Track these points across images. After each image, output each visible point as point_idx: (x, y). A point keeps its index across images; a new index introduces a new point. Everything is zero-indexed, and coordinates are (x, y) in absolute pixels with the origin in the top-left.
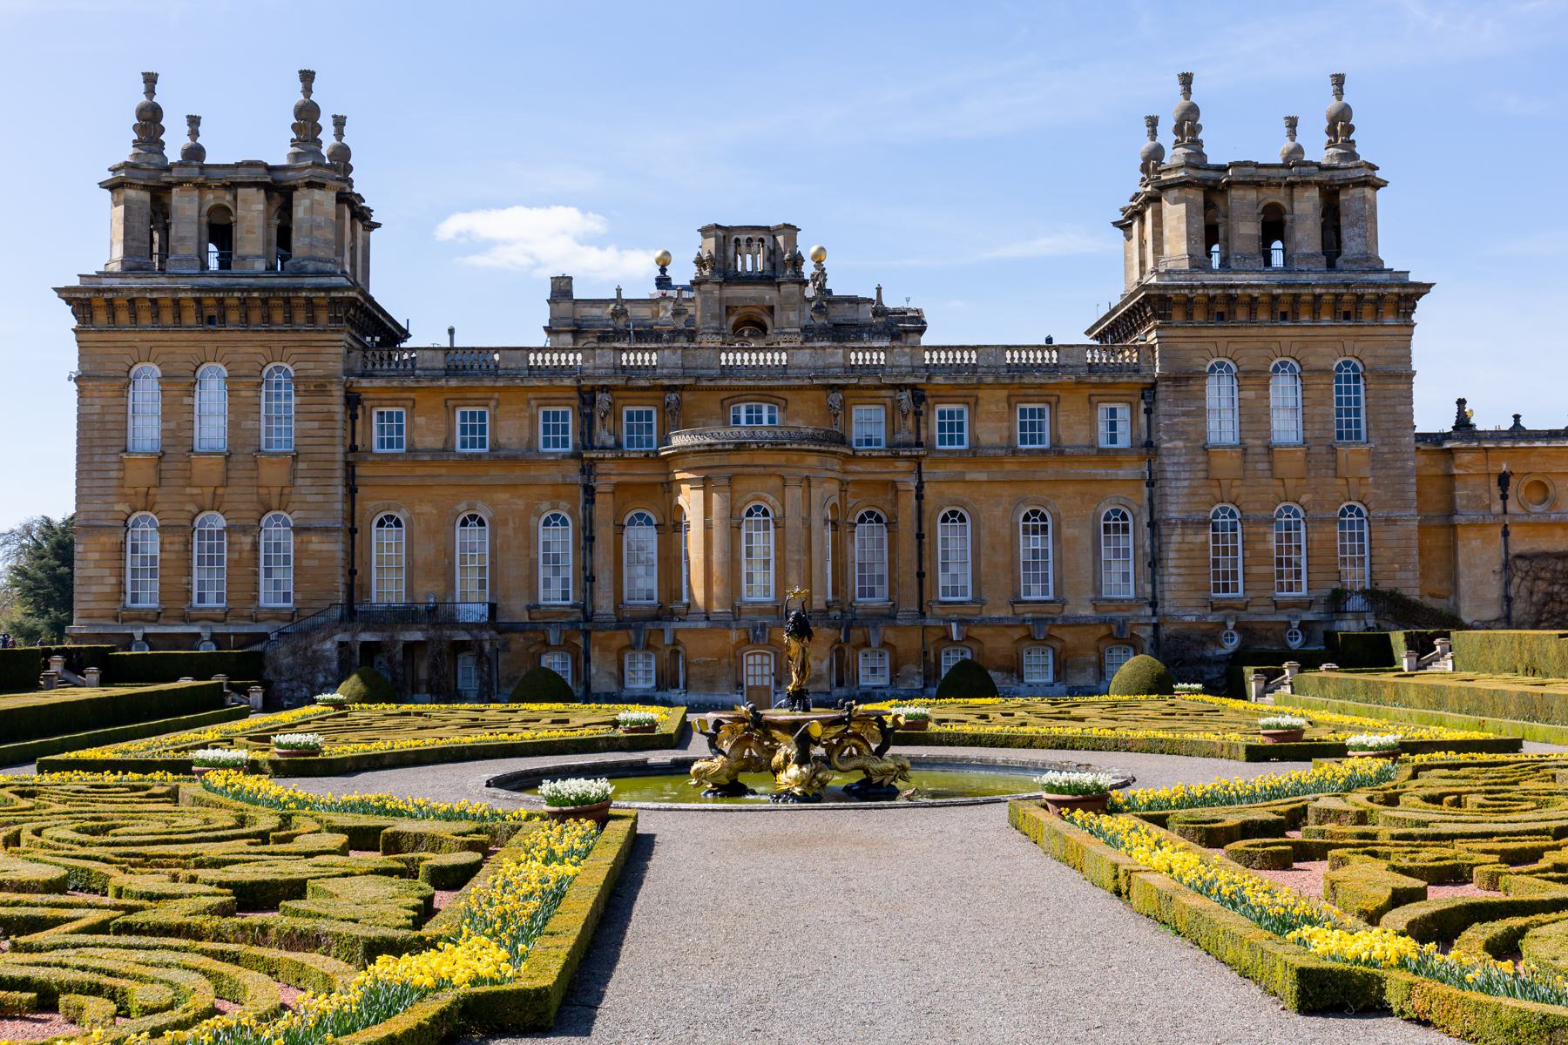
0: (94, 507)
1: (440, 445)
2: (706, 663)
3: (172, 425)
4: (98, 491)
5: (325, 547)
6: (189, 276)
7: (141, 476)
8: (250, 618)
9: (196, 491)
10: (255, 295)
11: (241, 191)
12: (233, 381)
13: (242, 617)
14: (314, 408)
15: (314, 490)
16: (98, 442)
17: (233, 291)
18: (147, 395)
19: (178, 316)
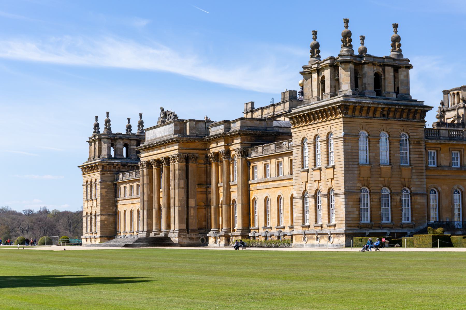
0: (350, 185)
1: (448, 164)
4: (351, 179)
6: (371, 98)
7: (365, 173)
8: (400, 227)
9: (382, 179)
10: (380, 106)
11: (387, 68)
12: (390, 139)
13: (397, 226)
14: (417, 150)
15: (418, 180)
17: (396, 105)
18: (363, 143)
19: (374, 113)
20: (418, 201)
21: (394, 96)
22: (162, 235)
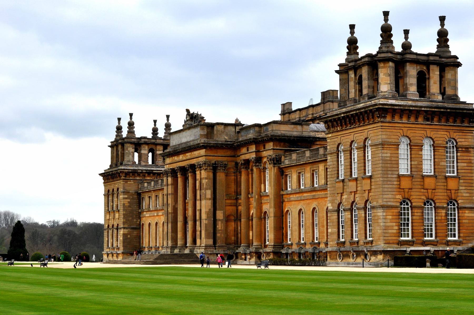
5: (470, 215)
11: (432, 67)
13: (442, 244)
14: (465, 158)
15: (466, 191)
16: (389, 169)
20: (466, 215)
21: (440, 98)
22: (187, 251)
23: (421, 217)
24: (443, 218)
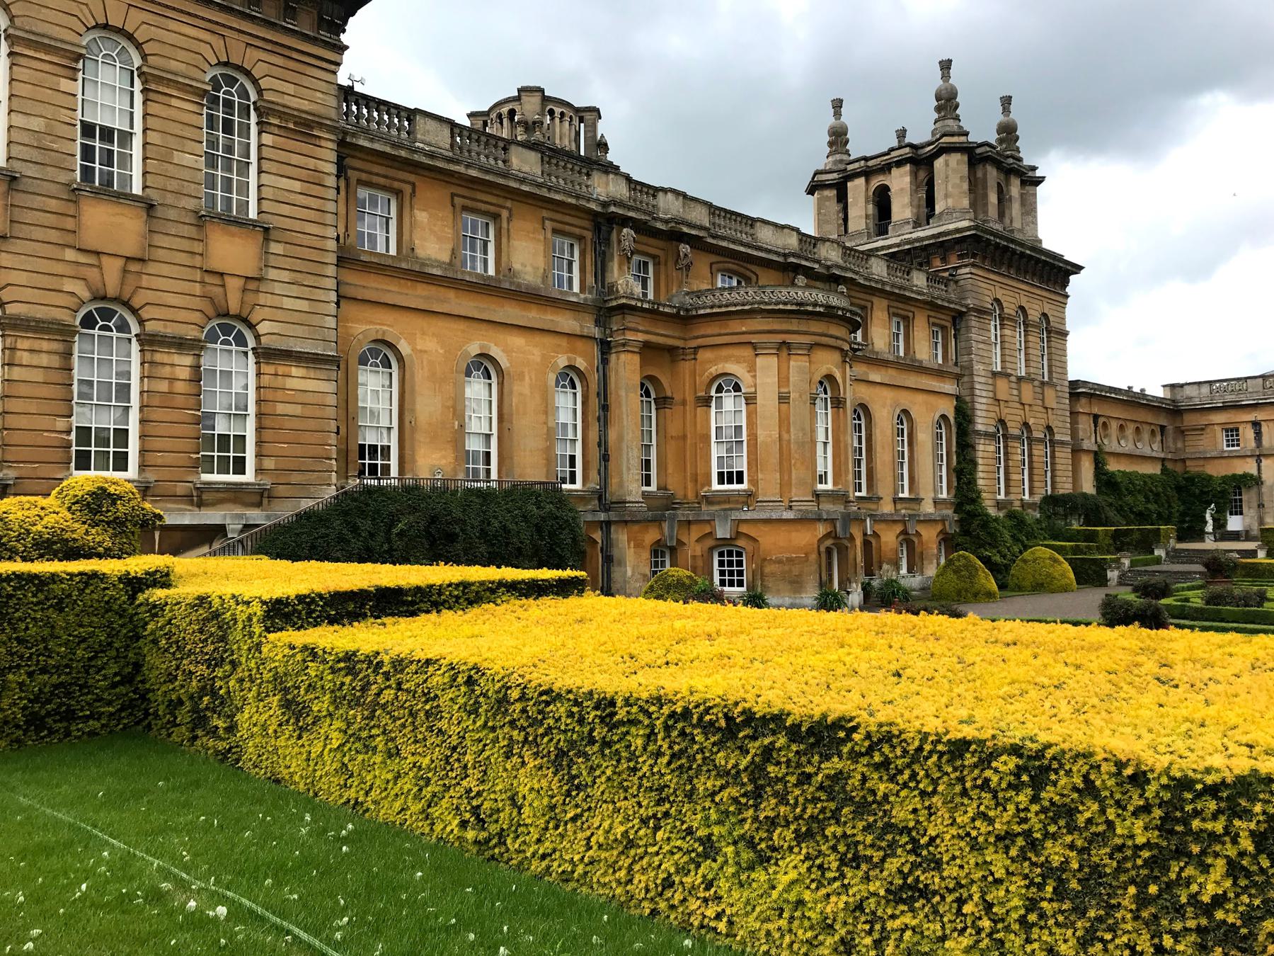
2: (790, 560)
3: (36, 124)
14: (295, 159)
23: (57, 377)
24: (180, 387)
